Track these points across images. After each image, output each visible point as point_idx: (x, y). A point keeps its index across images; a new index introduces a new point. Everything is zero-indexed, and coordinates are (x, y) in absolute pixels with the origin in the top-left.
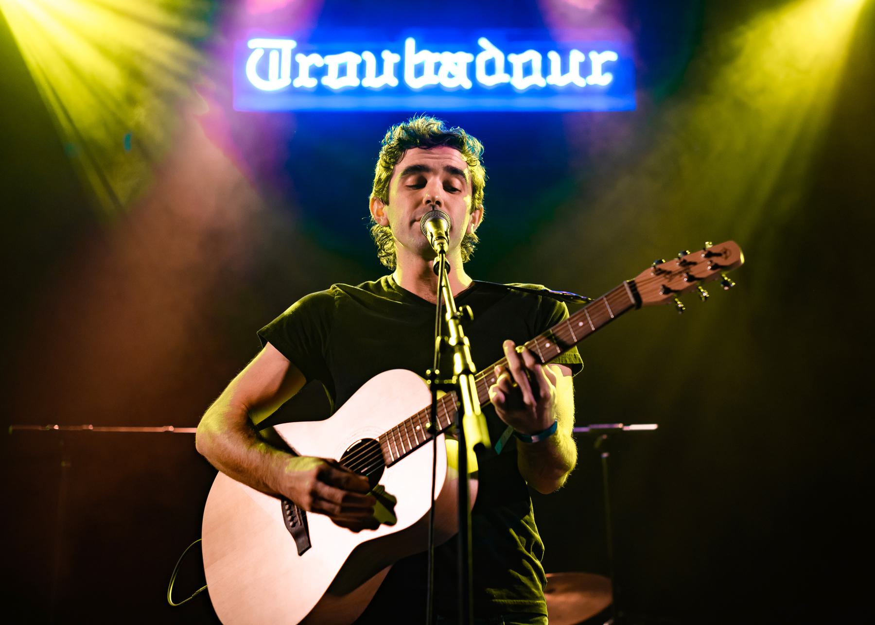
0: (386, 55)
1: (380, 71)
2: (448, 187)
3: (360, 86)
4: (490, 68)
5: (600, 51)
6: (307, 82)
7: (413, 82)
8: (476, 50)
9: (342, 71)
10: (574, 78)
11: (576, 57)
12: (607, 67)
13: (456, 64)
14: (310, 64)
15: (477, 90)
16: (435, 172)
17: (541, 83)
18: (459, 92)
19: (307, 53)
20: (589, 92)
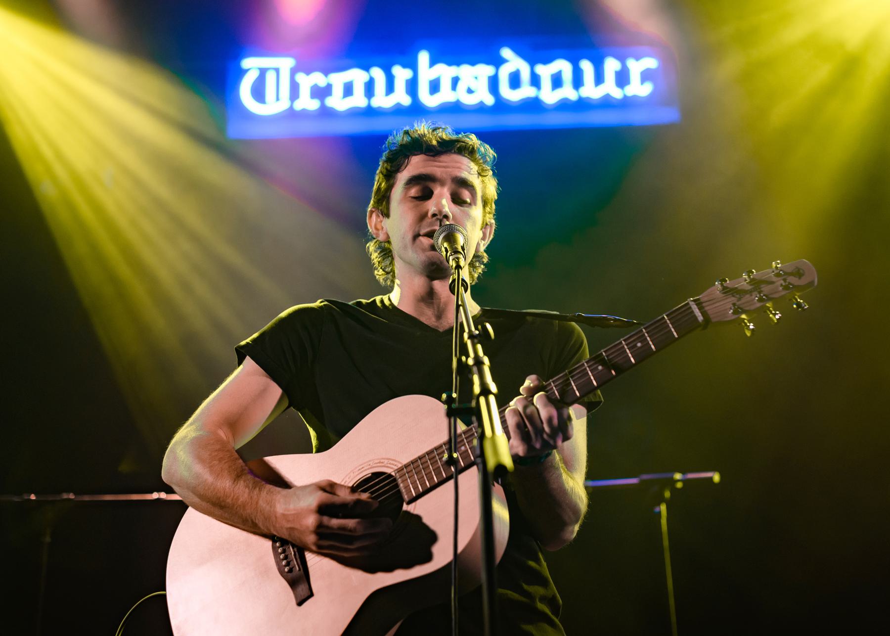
1: (390, 89)
2: (457, 200)
3: (369, 106)
4: (515, 81)
6: (307, 103)
7: (429, 101)
8: (498, 62)
9: (348, 90)
10: (610, 88)
11: (611, 65)
12: (646, 76)
13: (476, 78)
14: (312, 84)
15: (501, 106)
16: (442, 183)
18: (481, 108)
20: (627, 103)
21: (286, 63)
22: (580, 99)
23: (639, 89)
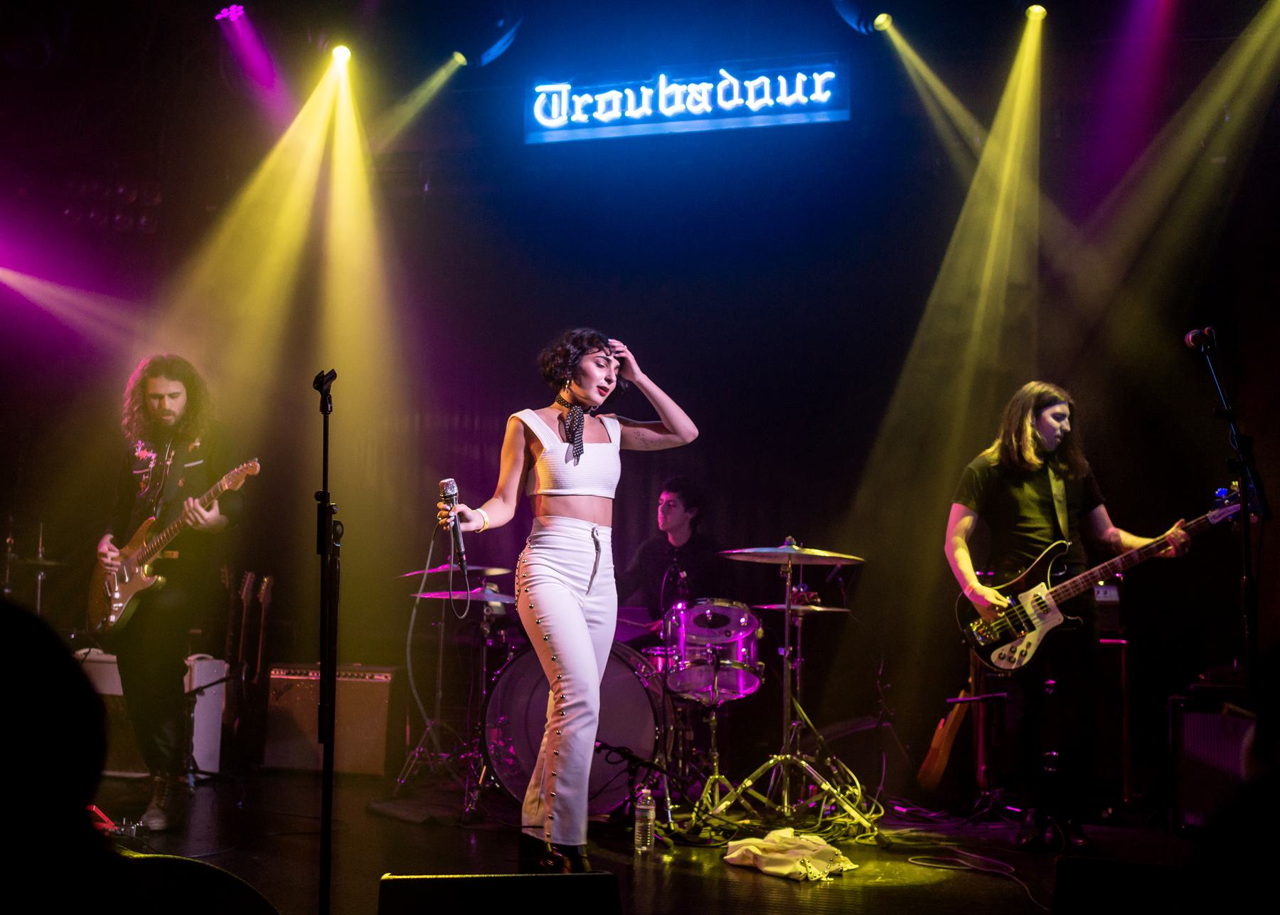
0: (643, 89)
1: (639, 103)
4: (728, 95)
5: (821, 72)
6: (579, 116)
8: (716, 79)
9: (609, 106)
10: (799, 97)
11: (801, 78)
12: (827, 86)
15: (718, 113)
17: (771, 103)
18: (704, 116)
19: (580, 94)
20: (812, 107)
21: (565, 88)
22: (776, 104)
23: (822, 96)
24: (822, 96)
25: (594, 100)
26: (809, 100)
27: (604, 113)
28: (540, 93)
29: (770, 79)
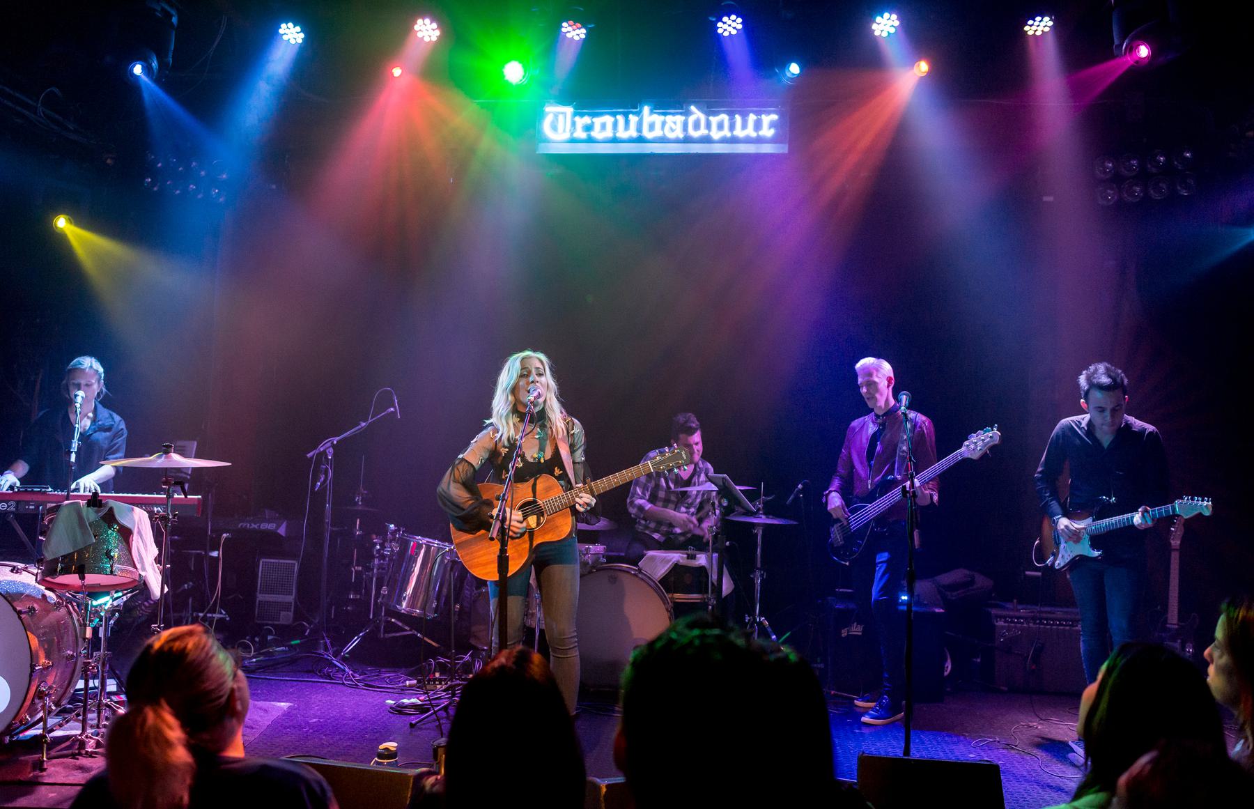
0: (631, 116)
4: (697, 126)
5: (768, 113)
7: (647, 134)
8: (687, 113)
9: (603, 126)
10: (750, 132)
11: (752, 118)
12: (772, 125)
15: (688, 140)
17: (729, 134)
18: (677, 141)
19: (582, 115)
20: (760, 140)
21: (569, 110)
24: (767, 132)
25: (593, 123)
26: (758, 134)
27: (600, 132)
28: (549, 113)
29: (728, 114)
